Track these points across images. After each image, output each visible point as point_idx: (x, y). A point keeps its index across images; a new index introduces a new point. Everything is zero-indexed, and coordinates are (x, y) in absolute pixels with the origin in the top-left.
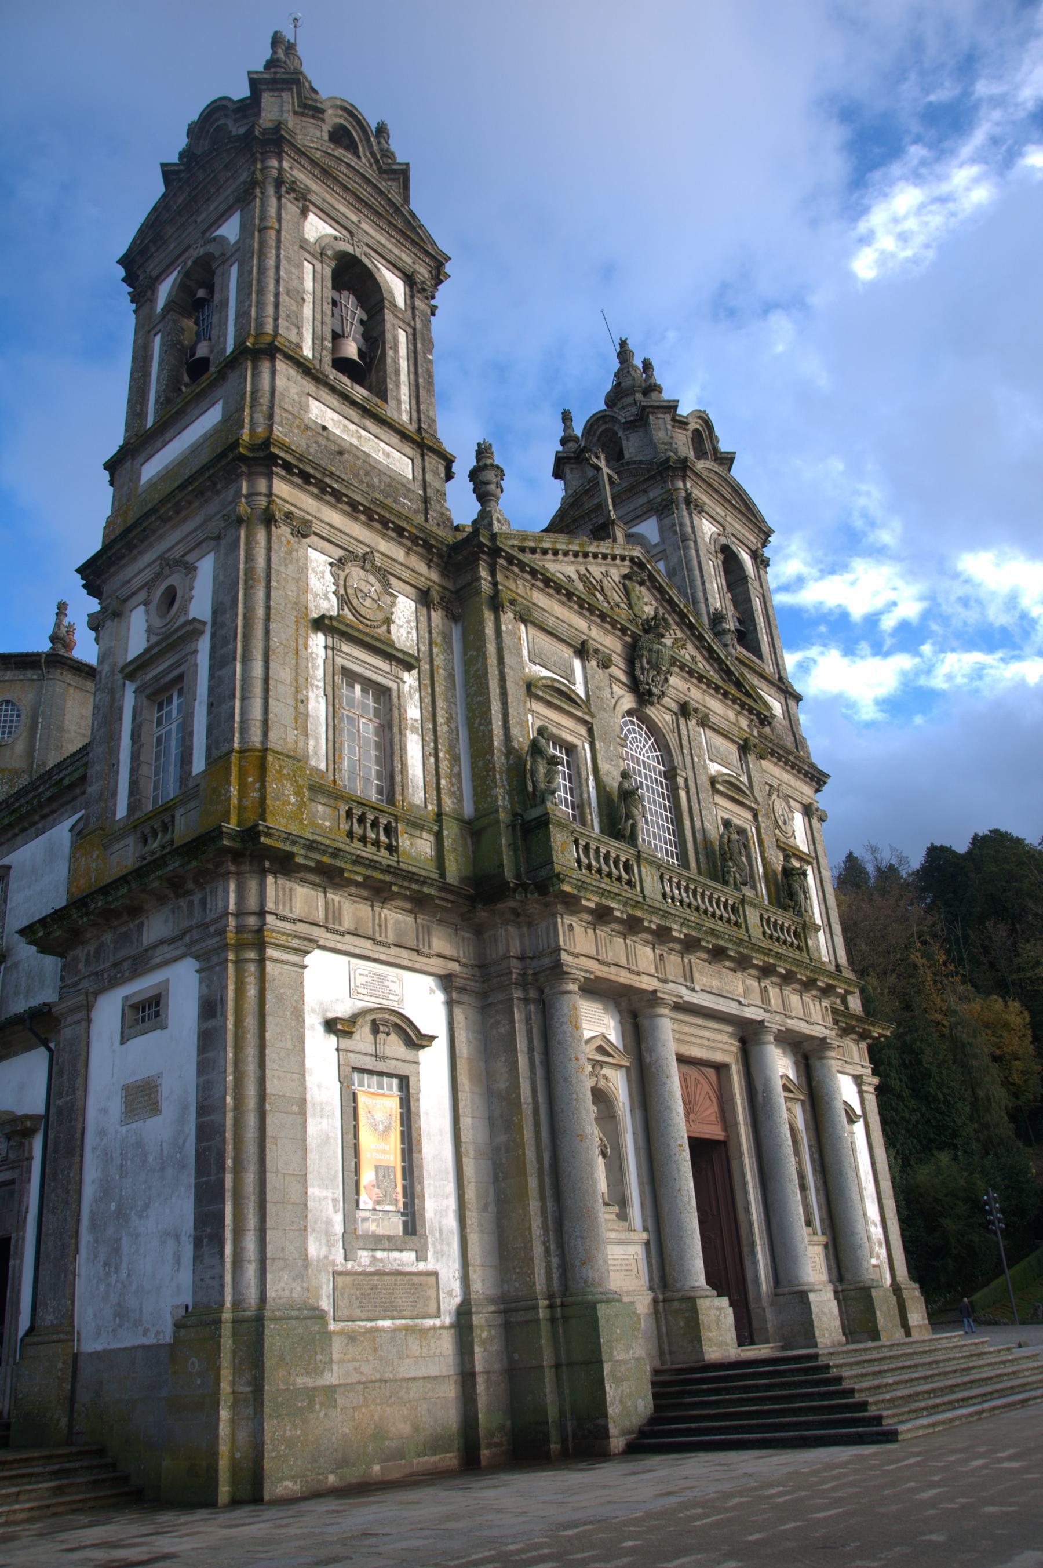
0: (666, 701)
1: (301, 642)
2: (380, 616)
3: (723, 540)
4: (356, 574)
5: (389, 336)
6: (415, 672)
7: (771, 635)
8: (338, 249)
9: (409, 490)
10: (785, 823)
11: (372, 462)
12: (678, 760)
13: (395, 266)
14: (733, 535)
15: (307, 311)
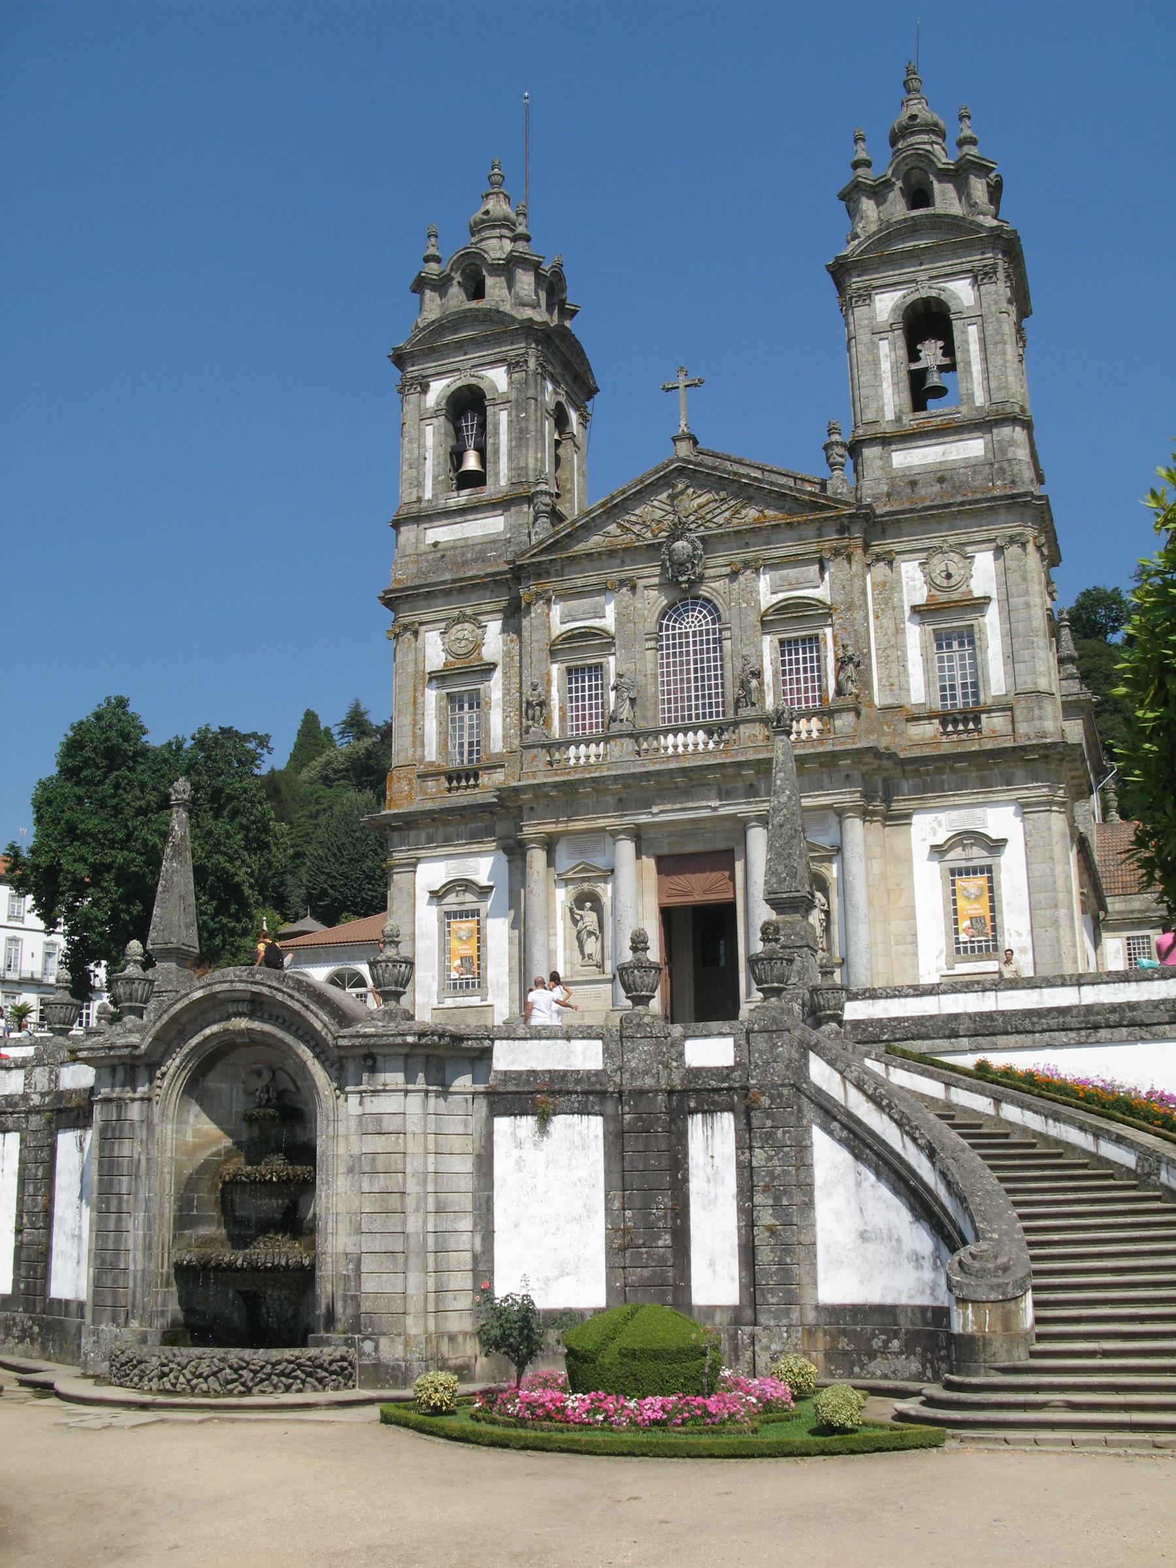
0: (709, 573)
1: (419, 694)
2: (471, 646)
3: (909, 300)
4: (456, 631)
5: (489, 428)
6: (499, 669)
7: (985, 360)
8: (449, 393)
9: (494, 542)
10: (949, 576)
11: (470, 542)
12: (725, 616)
13: (494, 363)
14: (932, 278)
15: (429, 465)
